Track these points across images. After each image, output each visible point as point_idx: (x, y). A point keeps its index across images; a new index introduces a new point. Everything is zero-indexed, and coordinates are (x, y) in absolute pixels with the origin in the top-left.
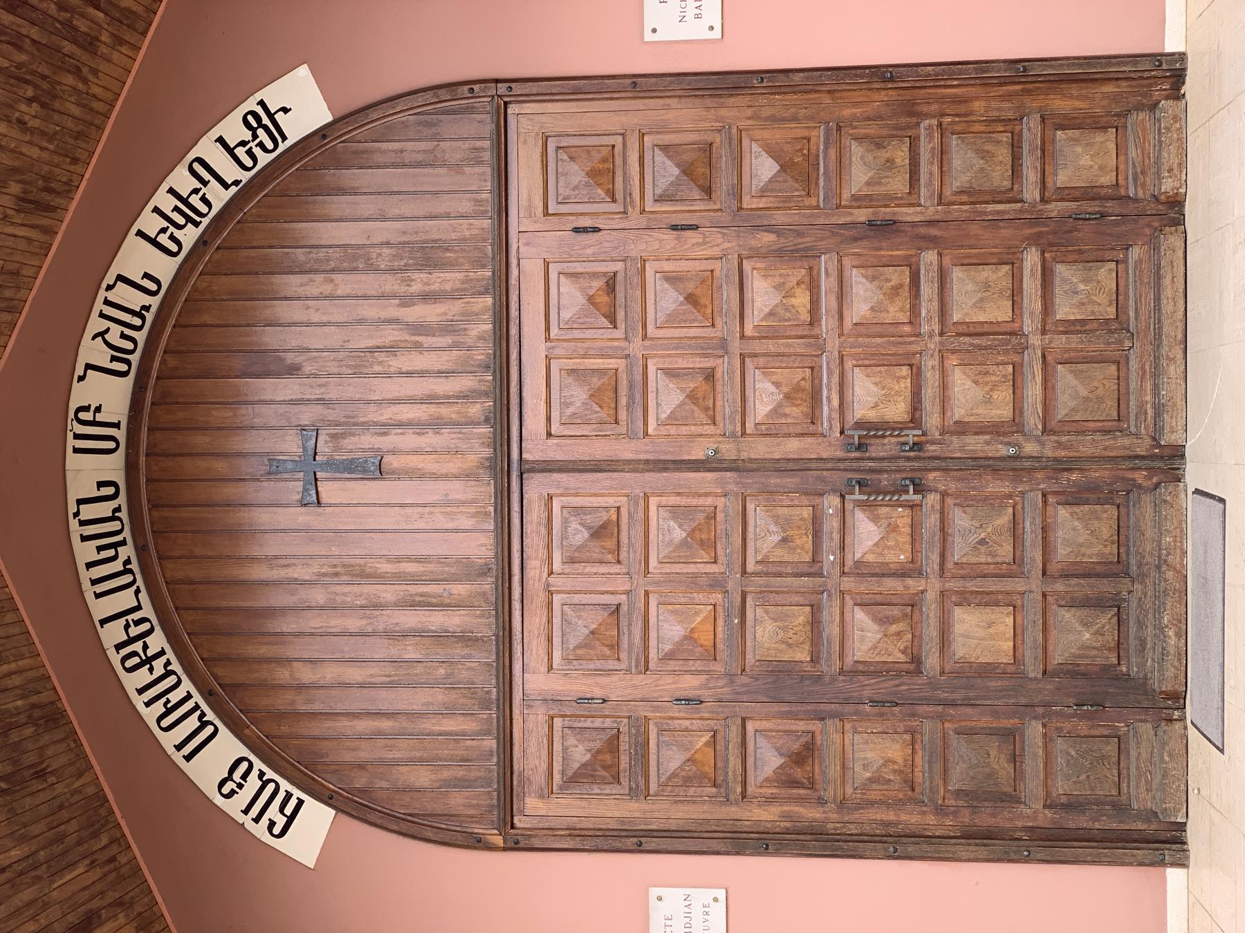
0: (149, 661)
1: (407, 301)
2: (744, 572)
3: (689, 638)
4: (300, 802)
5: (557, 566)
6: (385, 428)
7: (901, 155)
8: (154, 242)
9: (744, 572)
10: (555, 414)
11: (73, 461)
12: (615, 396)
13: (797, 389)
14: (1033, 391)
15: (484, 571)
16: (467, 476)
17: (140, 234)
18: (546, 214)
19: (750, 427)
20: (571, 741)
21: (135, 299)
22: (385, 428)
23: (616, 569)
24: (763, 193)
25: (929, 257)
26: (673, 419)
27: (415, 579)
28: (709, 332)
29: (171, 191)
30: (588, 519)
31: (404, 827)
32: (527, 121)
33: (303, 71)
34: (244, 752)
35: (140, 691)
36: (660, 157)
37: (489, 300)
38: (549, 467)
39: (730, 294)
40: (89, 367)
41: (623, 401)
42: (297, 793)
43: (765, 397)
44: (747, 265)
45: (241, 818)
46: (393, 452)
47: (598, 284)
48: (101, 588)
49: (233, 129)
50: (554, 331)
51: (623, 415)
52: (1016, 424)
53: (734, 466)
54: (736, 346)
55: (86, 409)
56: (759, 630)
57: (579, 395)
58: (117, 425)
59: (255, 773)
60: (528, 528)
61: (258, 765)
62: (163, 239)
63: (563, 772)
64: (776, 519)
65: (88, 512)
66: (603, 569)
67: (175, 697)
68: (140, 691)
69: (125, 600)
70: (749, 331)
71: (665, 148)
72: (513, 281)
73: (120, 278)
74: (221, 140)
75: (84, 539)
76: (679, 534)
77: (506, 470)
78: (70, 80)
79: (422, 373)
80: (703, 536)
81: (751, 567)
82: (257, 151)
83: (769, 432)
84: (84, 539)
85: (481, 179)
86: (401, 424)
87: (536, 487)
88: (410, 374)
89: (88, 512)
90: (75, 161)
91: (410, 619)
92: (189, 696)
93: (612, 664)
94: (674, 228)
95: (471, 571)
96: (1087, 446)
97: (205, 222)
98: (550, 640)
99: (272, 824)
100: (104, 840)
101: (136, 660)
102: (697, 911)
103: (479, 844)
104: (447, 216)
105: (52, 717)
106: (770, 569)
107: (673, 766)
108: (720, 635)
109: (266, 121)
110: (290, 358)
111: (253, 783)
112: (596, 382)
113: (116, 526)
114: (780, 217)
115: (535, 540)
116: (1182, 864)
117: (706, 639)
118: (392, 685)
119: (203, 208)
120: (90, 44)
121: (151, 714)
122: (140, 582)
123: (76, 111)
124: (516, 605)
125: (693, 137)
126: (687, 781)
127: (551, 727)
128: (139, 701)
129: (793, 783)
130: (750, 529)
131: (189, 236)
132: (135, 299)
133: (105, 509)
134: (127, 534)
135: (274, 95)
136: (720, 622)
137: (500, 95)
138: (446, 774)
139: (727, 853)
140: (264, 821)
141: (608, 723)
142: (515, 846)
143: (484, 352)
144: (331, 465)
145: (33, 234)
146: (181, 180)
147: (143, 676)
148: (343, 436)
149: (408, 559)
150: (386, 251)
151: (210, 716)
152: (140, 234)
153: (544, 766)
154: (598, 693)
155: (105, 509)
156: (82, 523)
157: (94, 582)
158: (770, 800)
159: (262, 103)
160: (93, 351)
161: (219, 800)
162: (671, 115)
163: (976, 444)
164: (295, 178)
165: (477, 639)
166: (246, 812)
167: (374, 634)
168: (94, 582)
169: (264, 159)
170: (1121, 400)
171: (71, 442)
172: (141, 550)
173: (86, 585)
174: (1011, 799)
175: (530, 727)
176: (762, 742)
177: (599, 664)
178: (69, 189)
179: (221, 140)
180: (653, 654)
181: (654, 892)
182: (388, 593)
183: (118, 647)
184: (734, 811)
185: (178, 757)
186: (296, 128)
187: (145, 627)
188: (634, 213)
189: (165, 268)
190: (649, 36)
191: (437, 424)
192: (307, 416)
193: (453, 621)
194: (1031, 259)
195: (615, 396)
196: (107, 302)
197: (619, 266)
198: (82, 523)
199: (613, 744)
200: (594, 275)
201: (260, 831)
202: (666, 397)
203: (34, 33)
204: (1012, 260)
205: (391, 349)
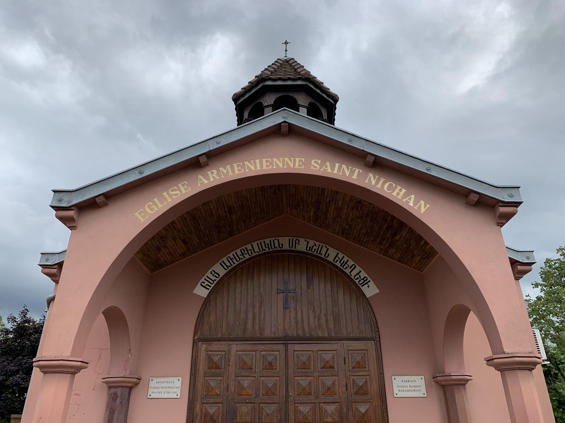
0: (243, 255)
1: (326, 315)
2: (260, 403)
3: (244, 388)
4: (208, 289)
5: (262, 353)
6: (296, 309)
8: (336, 256)
9: (260, 403)
10: (299, 353)
11: (287, 238)
12: (304, 367)
13: (307, 418)
15: (261, 334)
16: (284, 329)
17: (338, 253)
18: (348, 350)
19: (297, 405)
20: (219, 357)
21: (323, 252)
22: (296, 309)
23: (261, 369)
24: (357, 409)
26: (298, 384)
27: (260, 316)
28: (321, 393)
29: (348, 260)
30: (274, 361)
31: (201, 314)
32: (370, 345)
33: (378, 291)
34: (221, 276)
35: (236, 253)
36: (364, 380)
37: (327, 336)
38: (286, 351)
39: (330, 399)
40: (308, 242)
41: (303, 370)
42: (210, 288)
43: (304, 409)
44: (338, 404)
45: (206, 275)
46: (290, 311)
47: (332, 364)
48: (259, 244)
49: (363, 274)
50: (320, 352)
51: (299, 370)
53: (287, 401)
54: (317, 401)
55: (299, 241)
56: (245, 407)
57: (304, 359)
58: (295, 248)
59: (216, 278)
60: (271, 345)
61: (218, 279)
62: (337, 258)
63: (211, 354)
64: (273, 412)
65: (276, 242)
66: (261, 365)
67: (234, 260)
68: (236, 253)
69: (257, 250)
70: (321, 404)
71: (366, 382)
72: (332, 342)
73: (328, 249)
74: (360, 272)
75: (270, 241)
76: (270, 385)
77: (286, 340)
78: (372, 239)
79: (309, 319)
80: (269, 392)
81: (261, 405)
82: (358, 280)
83: (296, 410)
84: (270, 241)
85: (355, 334)
86: (296, 313)
87: (281, 347)
88: (308, 315)
89: (276, 242)
90: (353, 240)
91: (250, 315)
92: (234, 263)
93: (238, 367)
94: (346, 384)
97: (342, 268)
98: (244, 351)
99: (204, 283)
100: (203, 245)
101: (243, 251)
102: (175, 390)
103: (195, 333)
104: (346, 325)
105: (231, 234)
107: (212, 384)
108: (244, 396)
109: (366, 282)
110: (311, 287)
111: (213, 278)
112: (307, 363)
113: (273, 247)
114: (350, 414)
115: (268, 347)
117: (244, 392)
118: (235, 311)
119: (345, 267)
120: (380, 243)
121: (231, 255)
122: (260, 253)
123: (365, 240)
124: (253, 342)
125: (369, 389)
126: (207, 387)
127: (222, 351)
128: (234, 253)
129: (205, 417)
130: (271, 405)
131: (338, 264)
132: (323, 252)
133: (277, 245)
134: (271, 250)
135: (371, 284)
136: (247, 397)
137: (377, 339)
138: (213, 324)
139: (189, 398)
140: (205, 281)
141: (223, 366)
142: (194, 342)
143: (314, 334)
144: (287, 296)
145: (337, 231)
146: (351, 263)
147: (239, 253)
148: (294, 299)
149: (264, 315)
150: (337, 310)
151: (230, 268)
152: (338, 253)
153: (213, 350)
154: (231, 364)
155: (277, 245)
156: (274, 241)
157: (261, 243)
158: (201, 410)
159: (370, 281)
160: (311, 243)
161: (210, 271)
162: (374, 383)
164: (354, 289)
165: (245, 332)
166: (207, 277)
167: (247, 306)
168: (261, 243)
169: (357, 281)
171: (291, 238)
172: (268, 253)
173: (260, 241)
176: (216, 408)
177: (238, 364)
178: (347, 238)
179: (360, 272)
180: (240, 378)
181: (180, 378)
182: (256, 310)
183: (246, 248)
184: (199, 400)
185: (221, 261)
186: (364, 289)
187: (250, 254)
188: (349, 373)
189: (331, 259)
190: (393, 377)
191: (297, 322)
192: (298, 290)
193: (249, 326)
195: (304, 367)
196: (322, 246)
197: (336, 369)
198: (274, 241)
199: (218, 367)
200: (334, 363)
201: (203, 280)
203: (382, 232)
205: (314, 311)
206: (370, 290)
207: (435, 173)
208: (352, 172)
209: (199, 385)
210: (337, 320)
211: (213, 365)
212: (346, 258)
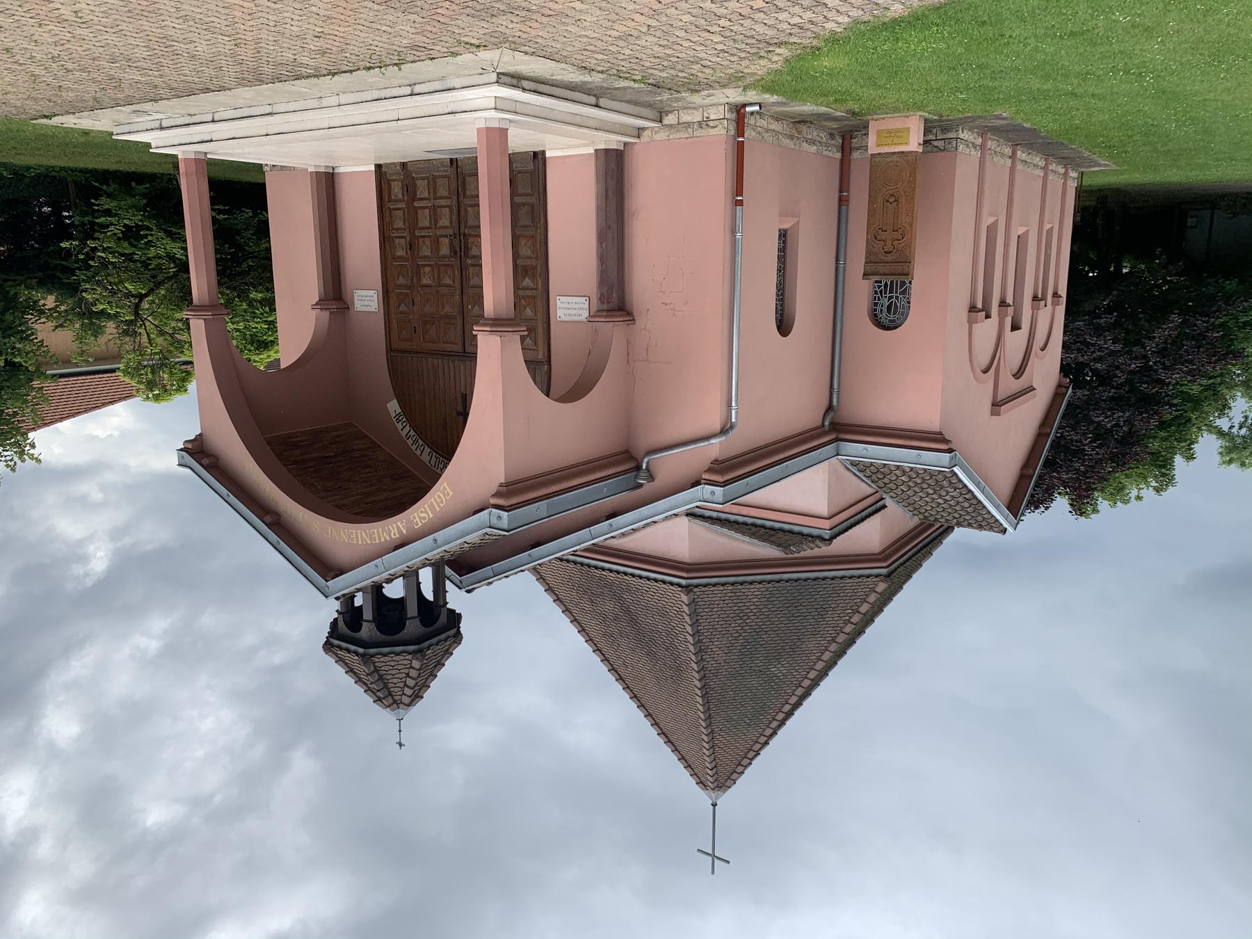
7: (397, 241)
14: (443, 202)
25: (417, 233)
32: (395, 345)
49: (399, 426)
52: (449, 207)
96: (454, 186)
116: (544, 152)
146: (410, 442)
163: (454, 217)
170: (443, 177)
174: (532, 206)
186: (399, 410)
189: (427, 450)
194: (416, 204)
204: (416, 209)
206: (393, 407)
207: (224, 491)
212: (414, 447)
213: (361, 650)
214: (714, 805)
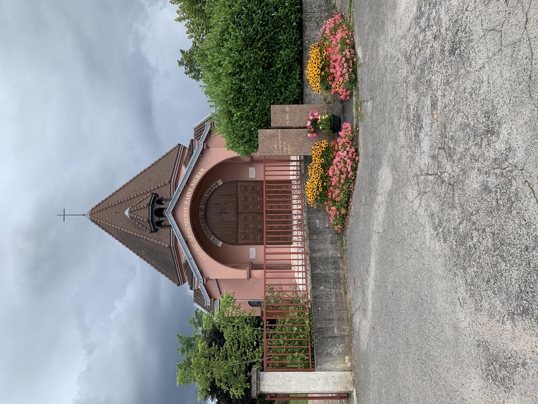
32: (239, 184)
49: (214, 184)
77: (237, 213)
83: (259, 210)
95: (234, 221)
103: (235, 245)
106: (259, 221)
146: (210, 189)
160: (201, 203)
175: (239, 235)
189: (208, 196)
193: (233, 226)
202: (251, 207)
208: (190, 191)
209: (252, 242)
210: (231, 195)
211: (246, 238)
213: (150, 219)
214: (84, 215)
